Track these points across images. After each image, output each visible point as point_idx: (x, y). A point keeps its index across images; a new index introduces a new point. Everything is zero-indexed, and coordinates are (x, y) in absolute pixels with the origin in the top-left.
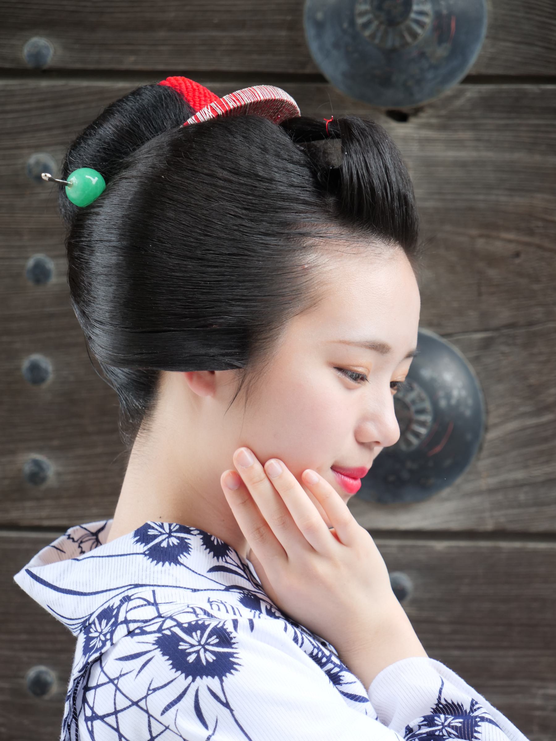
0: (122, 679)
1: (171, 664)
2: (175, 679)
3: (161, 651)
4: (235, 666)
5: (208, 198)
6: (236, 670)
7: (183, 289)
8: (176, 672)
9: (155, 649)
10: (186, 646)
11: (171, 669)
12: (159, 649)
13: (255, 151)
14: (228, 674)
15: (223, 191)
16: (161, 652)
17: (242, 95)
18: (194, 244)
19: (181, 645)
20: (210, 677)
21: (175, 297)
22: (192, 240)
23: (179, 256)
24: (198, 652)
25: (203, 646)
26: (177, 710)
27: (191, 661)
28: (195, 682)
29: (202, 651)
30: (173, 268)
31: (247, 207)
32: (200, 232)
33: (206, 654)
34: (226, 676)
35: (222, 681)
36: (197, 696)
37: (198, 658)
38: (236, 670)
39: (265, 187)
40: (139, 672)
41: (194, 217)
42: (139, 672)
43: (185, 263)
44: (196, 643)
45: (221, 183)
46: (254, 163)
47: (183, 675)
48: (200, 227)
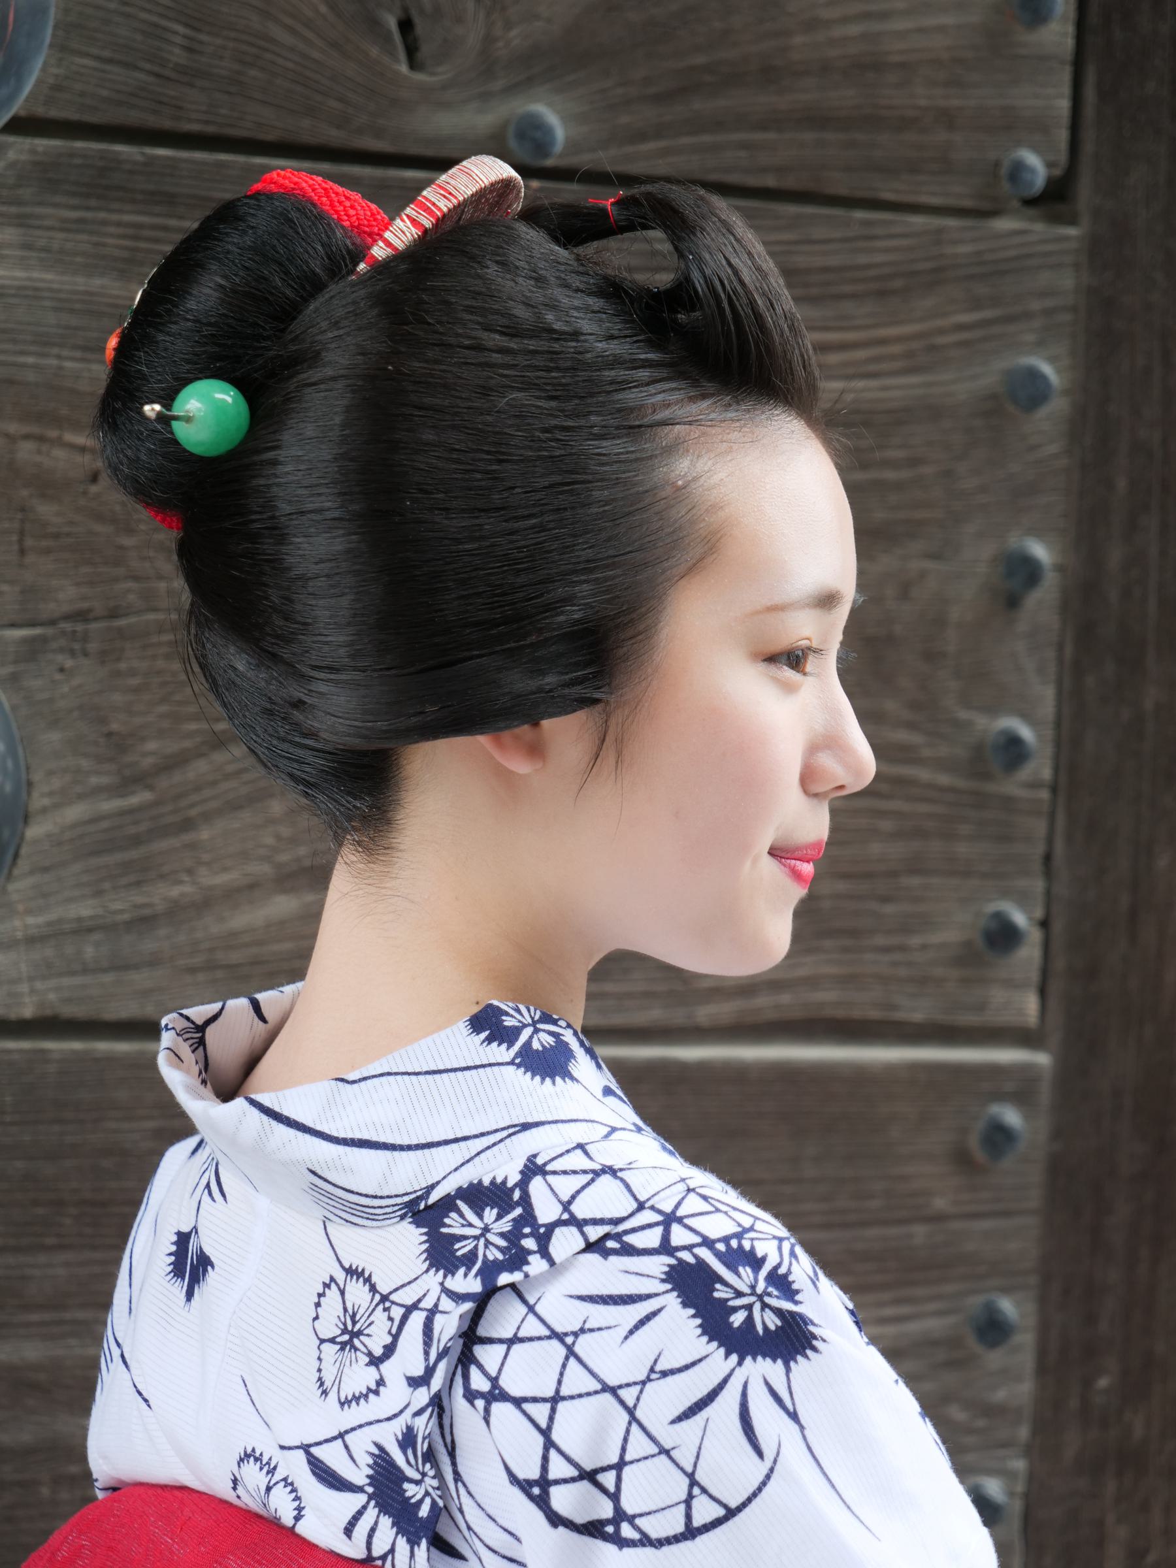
0: (582, 1339)
1: (700, 1326)
2: (707, 1356)
3: (678, 1296)
4: (815, 1342)
5: (485, 391)
6: (815, 1349)
7: (482, 573)
8: (708, 1343)
9: (667, 1292)
10: (727, 1292)
11: (699, 1336)
12: (675, 1294)
13: (525, 285)
14: (799, 1358)
15: (506, 372)
16: (680, 1300)
17: (452, 182)
18: (483, 483)
19: (718, 1290)
20: (768, 1360)
21: (471, 591)
22: (479, 476)
23: (463, 511)
24: (749, 1307)
25: (760, 1298)
26: (708, 1419)
27: (736, 1325)
28: (743, 1366)
29: (757, 1307)
30: (459, 536)
31: (554, 393)
32: (489, 457)
33: (764, 1313)
34: (796, 1362)
35: (788, 1370)
36: (744, 1394)
37: (750, 1319)
38: (815, 1349)
39: (572, 350)
40: (631, 1332)
41: (471, 432)
42: (631, 1332)
43: (477, 521)
44: (747, 1290)
45: (497, 358)
46: (536, 308)
47: (722, 1351)
48: (485, 448)
